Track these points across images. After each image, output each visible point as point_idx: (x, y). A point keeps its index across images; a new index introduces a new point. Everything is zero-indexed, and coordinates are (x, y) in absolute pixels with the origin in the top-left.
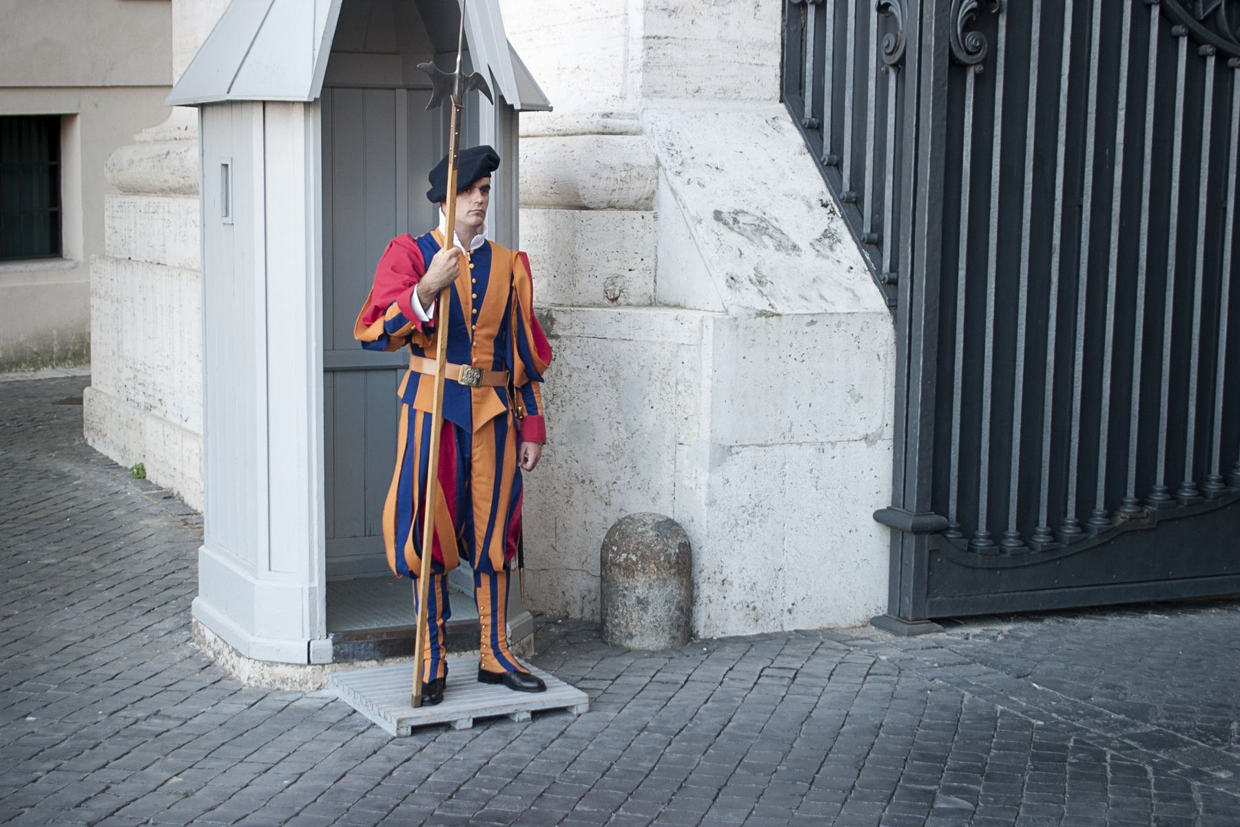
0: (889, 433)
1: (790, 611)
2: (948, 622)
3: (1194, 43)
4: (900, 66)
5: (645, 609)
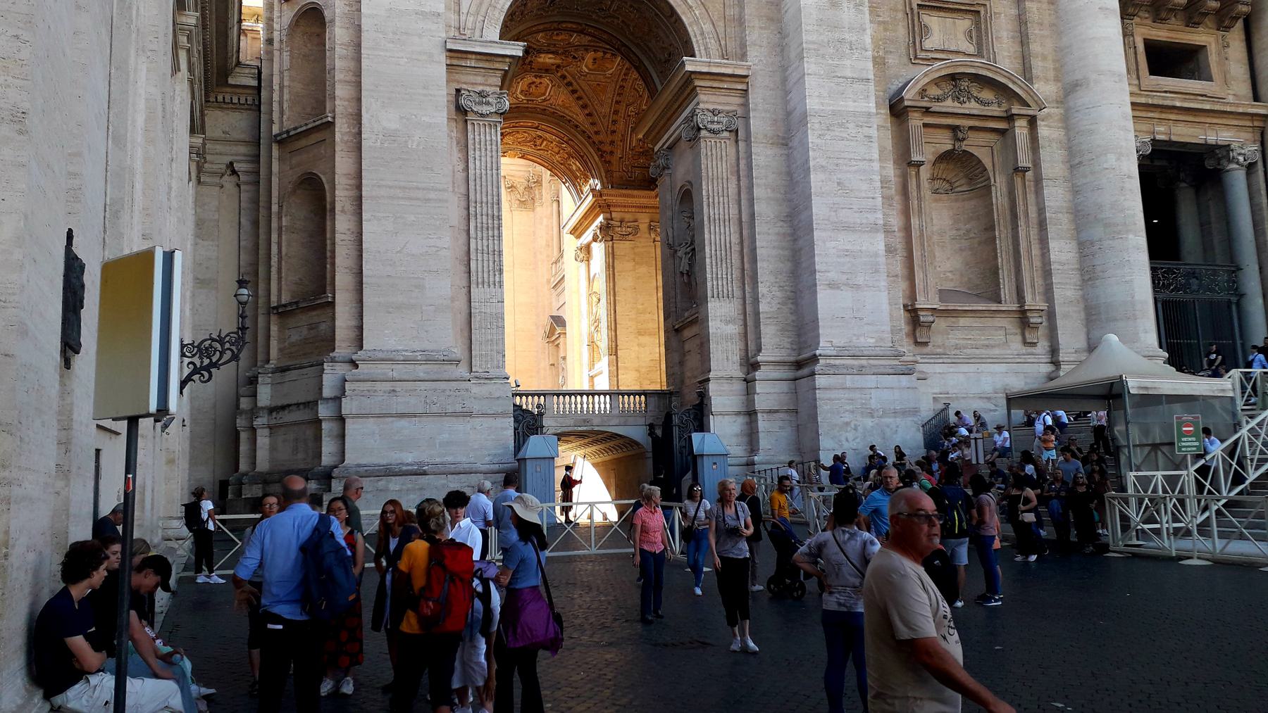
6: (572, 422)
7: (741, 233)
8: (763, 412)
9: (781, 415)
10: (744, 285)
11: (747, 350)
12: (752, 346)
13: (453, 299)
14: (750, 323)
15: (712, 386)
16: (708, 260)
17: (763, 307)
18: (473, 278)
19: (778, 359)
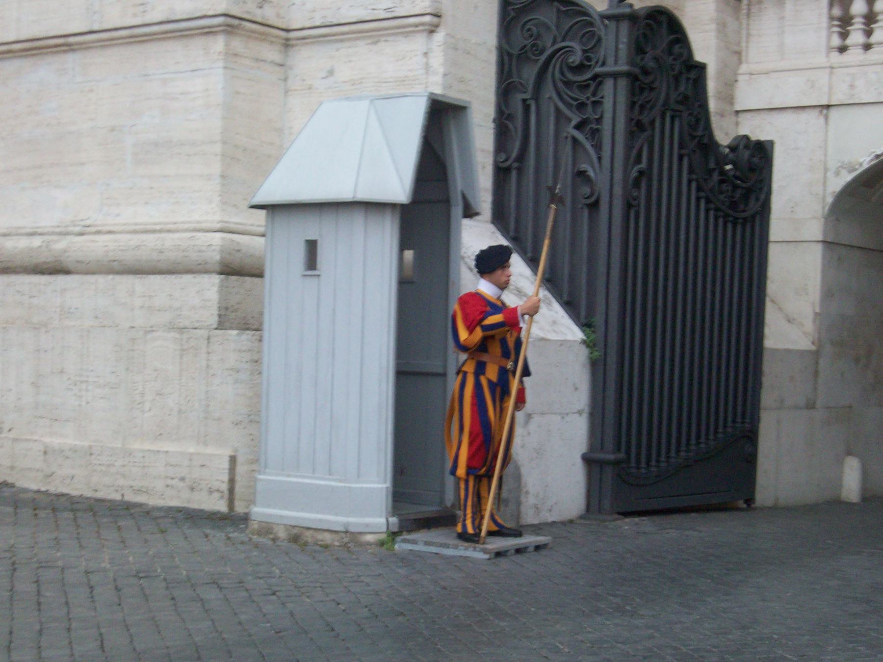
0: (587, 410)
1: (550, 510)
2: (626, 514)
3: (708, 201)
4: (594, 206)
5: (506, 505)
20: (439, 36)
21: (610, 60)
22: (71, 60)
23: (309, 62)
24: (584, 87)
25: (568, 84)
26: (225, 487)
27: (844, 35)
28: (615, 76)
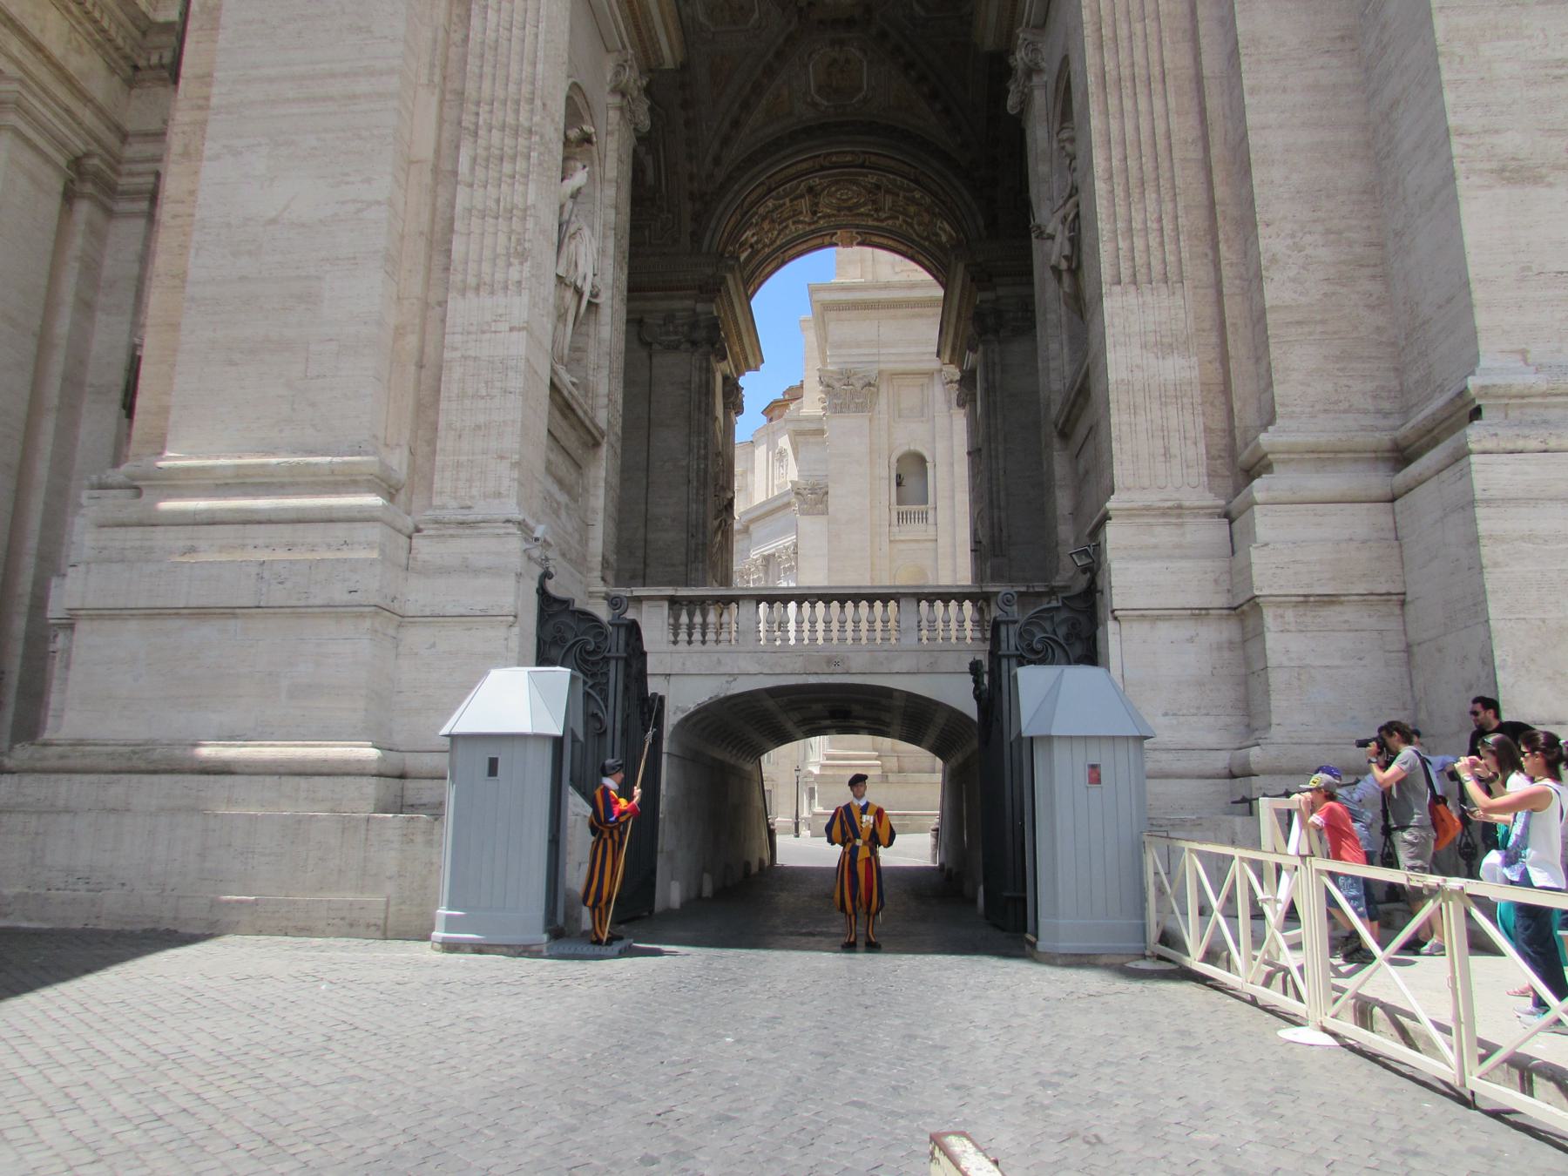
6: (798, 665)
7: (1202, 112)
8: (1282, 601)
9: (1349, 614)
10: (1215, 246)
11: (1231, 431)
12: (1246, 415)
13: (400, 332)
14: (1239, 349)
15: (1113, 534)
16: (1100, 187)
17: (1274, 293)
18: (456, 278)
19: (1324, 439)
20: (516, 630)
21: (614, 649)
22: (232, 624)
23: (415, 637)
24: (594, 663)
25: (585, 661)
26: (381, 922)
27: (676, 635)
28: (617, 659)
